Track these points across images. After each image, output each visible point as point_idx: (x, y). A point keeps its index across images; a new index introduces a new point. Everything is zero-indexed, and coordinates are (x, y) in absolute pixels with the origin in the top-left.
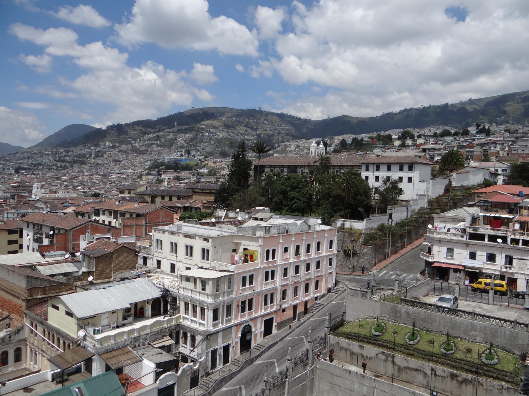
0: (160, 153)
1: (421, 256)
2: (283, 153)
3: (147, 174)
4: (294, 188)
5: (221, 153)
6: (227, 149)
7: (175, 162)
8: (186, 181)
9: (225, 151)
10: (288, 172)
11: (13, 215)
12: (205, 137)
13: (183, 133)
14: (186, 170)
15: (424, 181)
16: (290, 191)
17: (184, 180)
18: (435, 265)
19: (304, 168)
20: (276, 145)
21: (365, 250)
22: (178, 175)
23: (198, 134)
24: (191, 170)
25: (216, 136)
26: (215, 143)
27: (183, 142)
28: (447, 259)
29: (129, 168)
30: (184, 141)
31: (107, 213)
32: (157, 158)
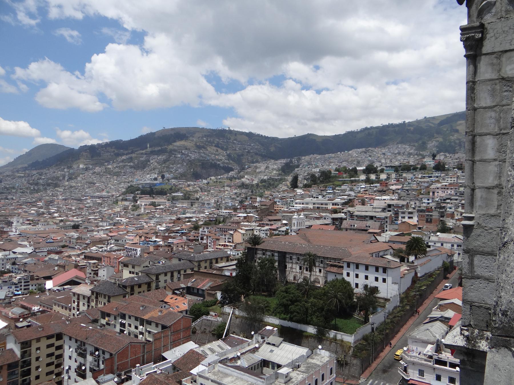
0: (134, 174)
1: (399, 372)
2: (253, 174)
3: (122, 200)
4: (293, 302)
5: (193, 174)
6: (199, 170)
7: (150, 187)
10: (278, 256)
11: (3, 261)
12: (177, 159)
15: (395, 283)
16: (290, 305)
18: (410, 383)
19: (293, 255)
20: (246, 167)
21: (355, 362)
22: (154, 200)
24: (166, 194)
26: (187, 165)
27: (156, 164)
28: (420, 378)
29: (103, 190)
30: (158, 163)
31: (133, 319)
32: (130, 180)
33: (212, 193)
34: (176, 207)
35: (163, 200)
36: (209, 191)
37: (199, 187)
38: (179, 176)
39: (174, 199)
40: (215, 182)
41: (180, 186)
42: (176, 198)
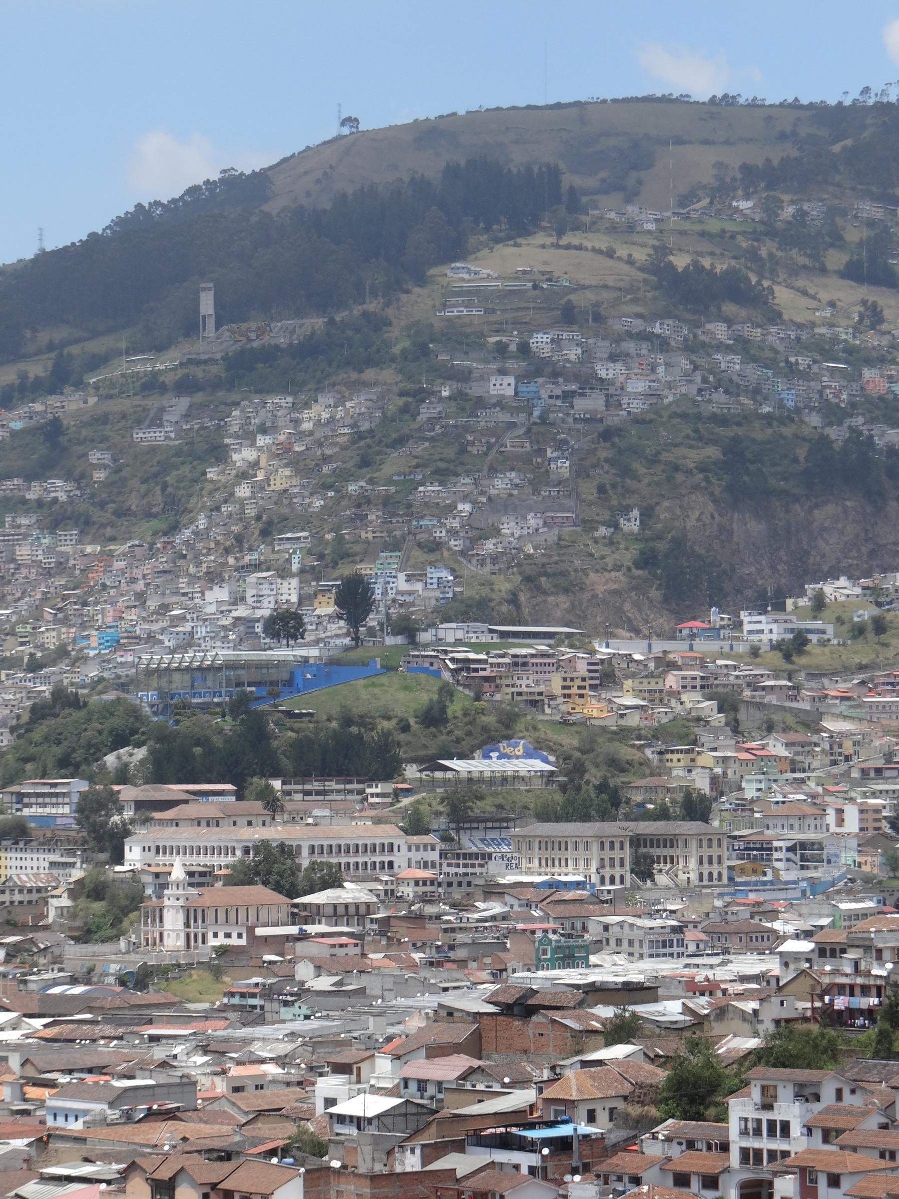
0: (78, 594)
5: (646, 560)
6: (696, 515)
7: (239, 706)
8: (352, 892)
9: (679, 543)
12: (485, 419)
13: (283, 390)
14: (343, 773)
17: (333, 881)
22: (275, 833)
23: (420, 395)
24: (388, 770)
25: (592, 403)
26: (581, 472)
27: (282, 478)
30: (297, 464)
32: (51, 639)
33: (836, 740)
34: (493, 891)
35: (360, 830)
36: (811, 723)
37: (706, 687)
38: (503, 585)
39: (467, 812)
40: (859, 631)
41: (526, 683)
42: (479, 808)
